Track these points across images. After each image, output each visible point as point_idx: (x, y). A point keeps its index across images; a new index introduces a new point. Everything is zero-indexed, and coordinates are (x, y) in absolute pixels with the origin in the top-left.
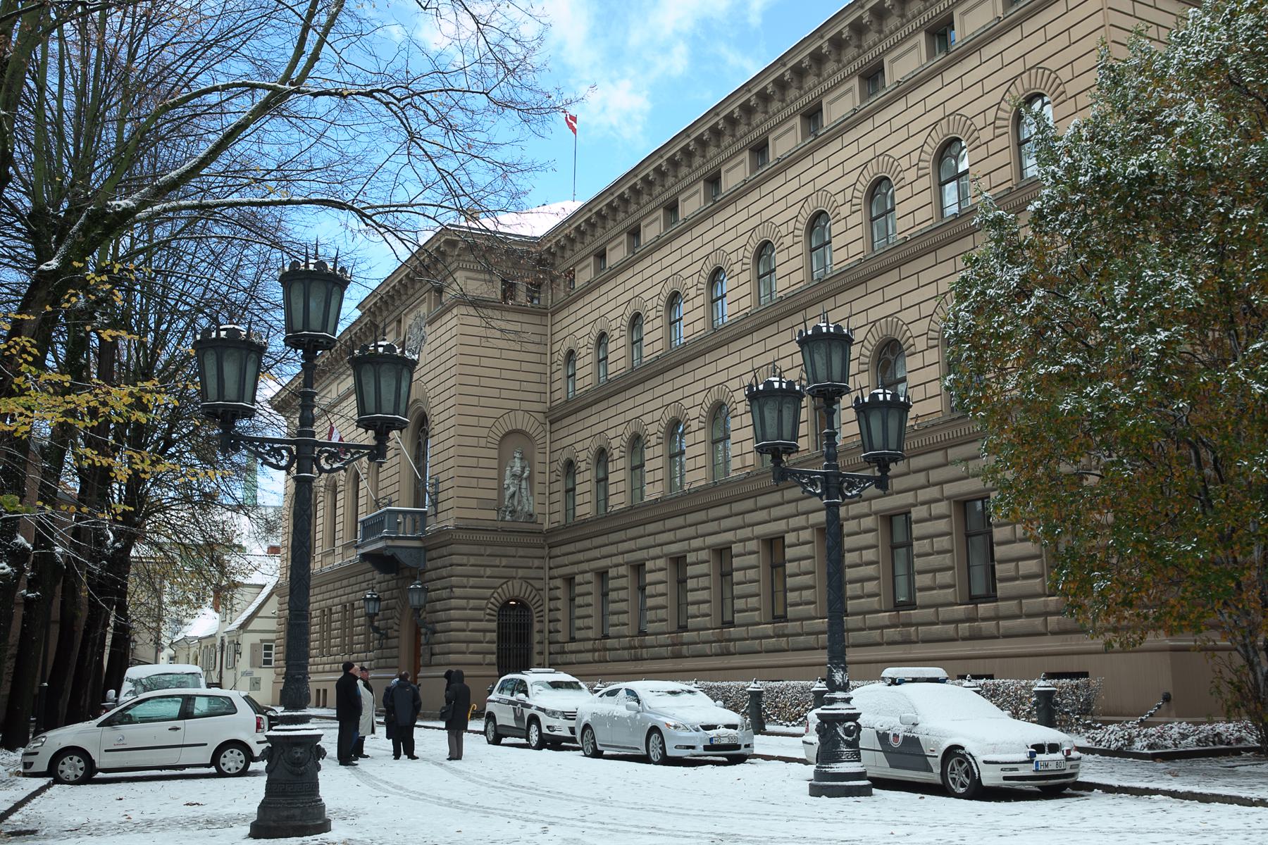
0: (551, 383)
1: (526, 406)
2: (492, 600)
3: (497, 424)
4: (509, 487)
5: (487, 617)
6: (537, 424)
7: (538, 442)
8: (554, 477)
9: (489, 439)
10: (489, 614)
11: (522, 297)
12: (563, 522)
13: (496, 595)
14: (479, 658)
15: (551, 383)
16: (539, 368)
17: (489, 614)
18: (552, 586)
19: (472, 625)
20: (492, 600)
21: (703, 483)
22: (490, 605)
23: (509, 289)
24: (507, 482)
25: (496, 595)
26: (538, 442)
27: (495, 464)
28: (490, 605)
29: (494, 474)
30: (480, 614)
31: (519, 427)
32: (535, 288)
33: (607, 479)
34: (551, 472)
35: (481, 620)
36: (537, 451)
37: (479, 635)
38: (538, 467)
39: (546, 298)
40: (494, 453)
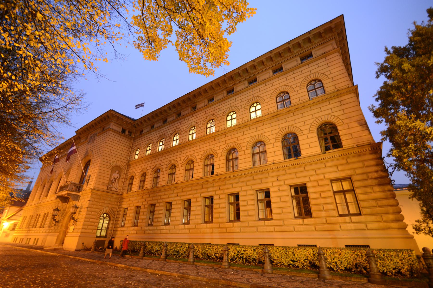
0: (130, 156)
1: (122, 160)
2: (100, 213)
5: (97, 218)
6: (124, 165)
10: (98, 217)
11: (127, 133)
13: (101, 211)
14: (90, 231)
15: (130, 156)
16: (128, 152)
17: (98, 217)
18: (119, 210)
19: (91, 220)
20: (100, 213)
21: (182, 181)
22: (98, 214)
23: (123, 131)
25: (101, 211)
27: (110, 174)
28: (98, 214)
29: (109, 176)
30: (94, 217)
32: (130, 133)
34: (125, 179)
35: (94, 219)
37: (93, 224)
38: (121, 177)
39: (133, 135)
40: (110, 171)
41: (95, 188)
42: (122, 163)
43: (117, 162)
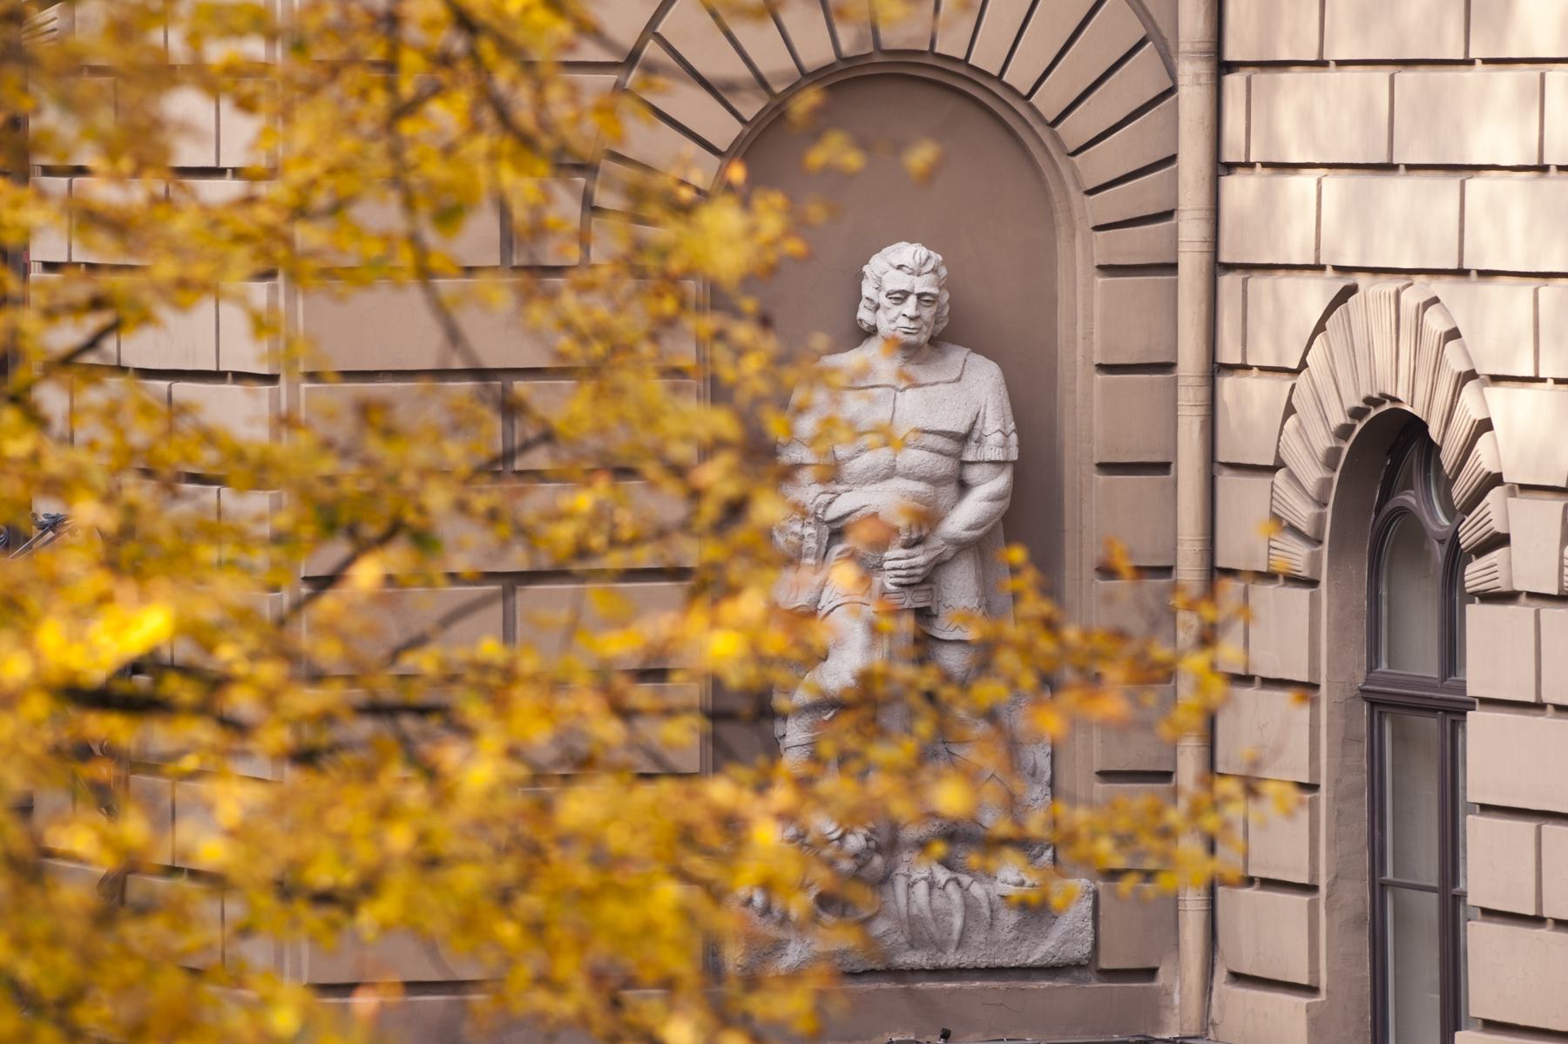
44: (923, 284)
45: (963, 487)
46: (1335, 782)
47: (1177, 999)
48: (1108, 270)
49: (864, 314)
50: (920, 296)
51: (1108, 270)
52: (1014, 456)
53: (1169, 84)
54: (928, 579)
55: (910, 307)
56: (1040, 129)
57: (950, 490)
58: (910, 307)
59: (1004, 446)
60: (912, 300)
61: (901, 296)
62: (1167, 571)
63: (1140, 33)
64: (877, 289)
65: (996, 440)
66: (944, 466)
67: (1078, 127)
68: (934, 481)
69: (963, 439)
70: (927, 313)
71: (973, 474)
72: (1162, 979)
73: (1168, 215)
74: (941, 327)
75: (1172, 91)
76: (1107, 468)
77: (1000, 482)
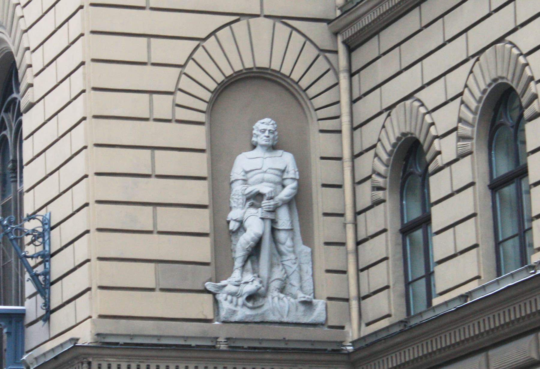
3: (200, 55)
4: (242, 227)
6: (310, 52)
7: (319, 102)
8: (365, 199)
9: (181, 98)
12: (399, 315)
24: (235, 214)
26: (319, 102)
31: (262, 62)
33: (523, 172)
34: (356, 183)
36: (315, 127)
41: (108, 327)
42: (282, 31)
43: (243, 22)
44: (270, 127)
45: (284, 186)
46: (394, 256)
47: (351, 334)
48: (322, 131)
49: (254, 139)
50: (269, 130)
51: (322, 131)
52: (298, 177)
53: (336, 82)
54: (274, 210)
55: (267, 133)
56: (301, 92)
57: (280, 187)
58: (267, 133)
59: (295, 174)
60: (267, 132)
61: (263, 131)
62: (342, 215)
63: (327, 67)
64: (217, 338)
65: (292, 172)
66: (278, 179)
67: (312, 92)
68: (276, 183)
69: (283, 171)
70: (271, 136)
71: (286, 182)
72: (347, 329)
73: (338, 102)
74: (275, 143)
75: (337, 84)
76: (324, 185)
77: (294, 184)
